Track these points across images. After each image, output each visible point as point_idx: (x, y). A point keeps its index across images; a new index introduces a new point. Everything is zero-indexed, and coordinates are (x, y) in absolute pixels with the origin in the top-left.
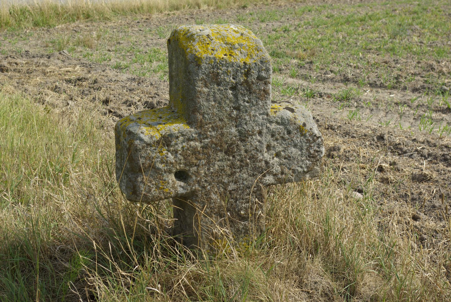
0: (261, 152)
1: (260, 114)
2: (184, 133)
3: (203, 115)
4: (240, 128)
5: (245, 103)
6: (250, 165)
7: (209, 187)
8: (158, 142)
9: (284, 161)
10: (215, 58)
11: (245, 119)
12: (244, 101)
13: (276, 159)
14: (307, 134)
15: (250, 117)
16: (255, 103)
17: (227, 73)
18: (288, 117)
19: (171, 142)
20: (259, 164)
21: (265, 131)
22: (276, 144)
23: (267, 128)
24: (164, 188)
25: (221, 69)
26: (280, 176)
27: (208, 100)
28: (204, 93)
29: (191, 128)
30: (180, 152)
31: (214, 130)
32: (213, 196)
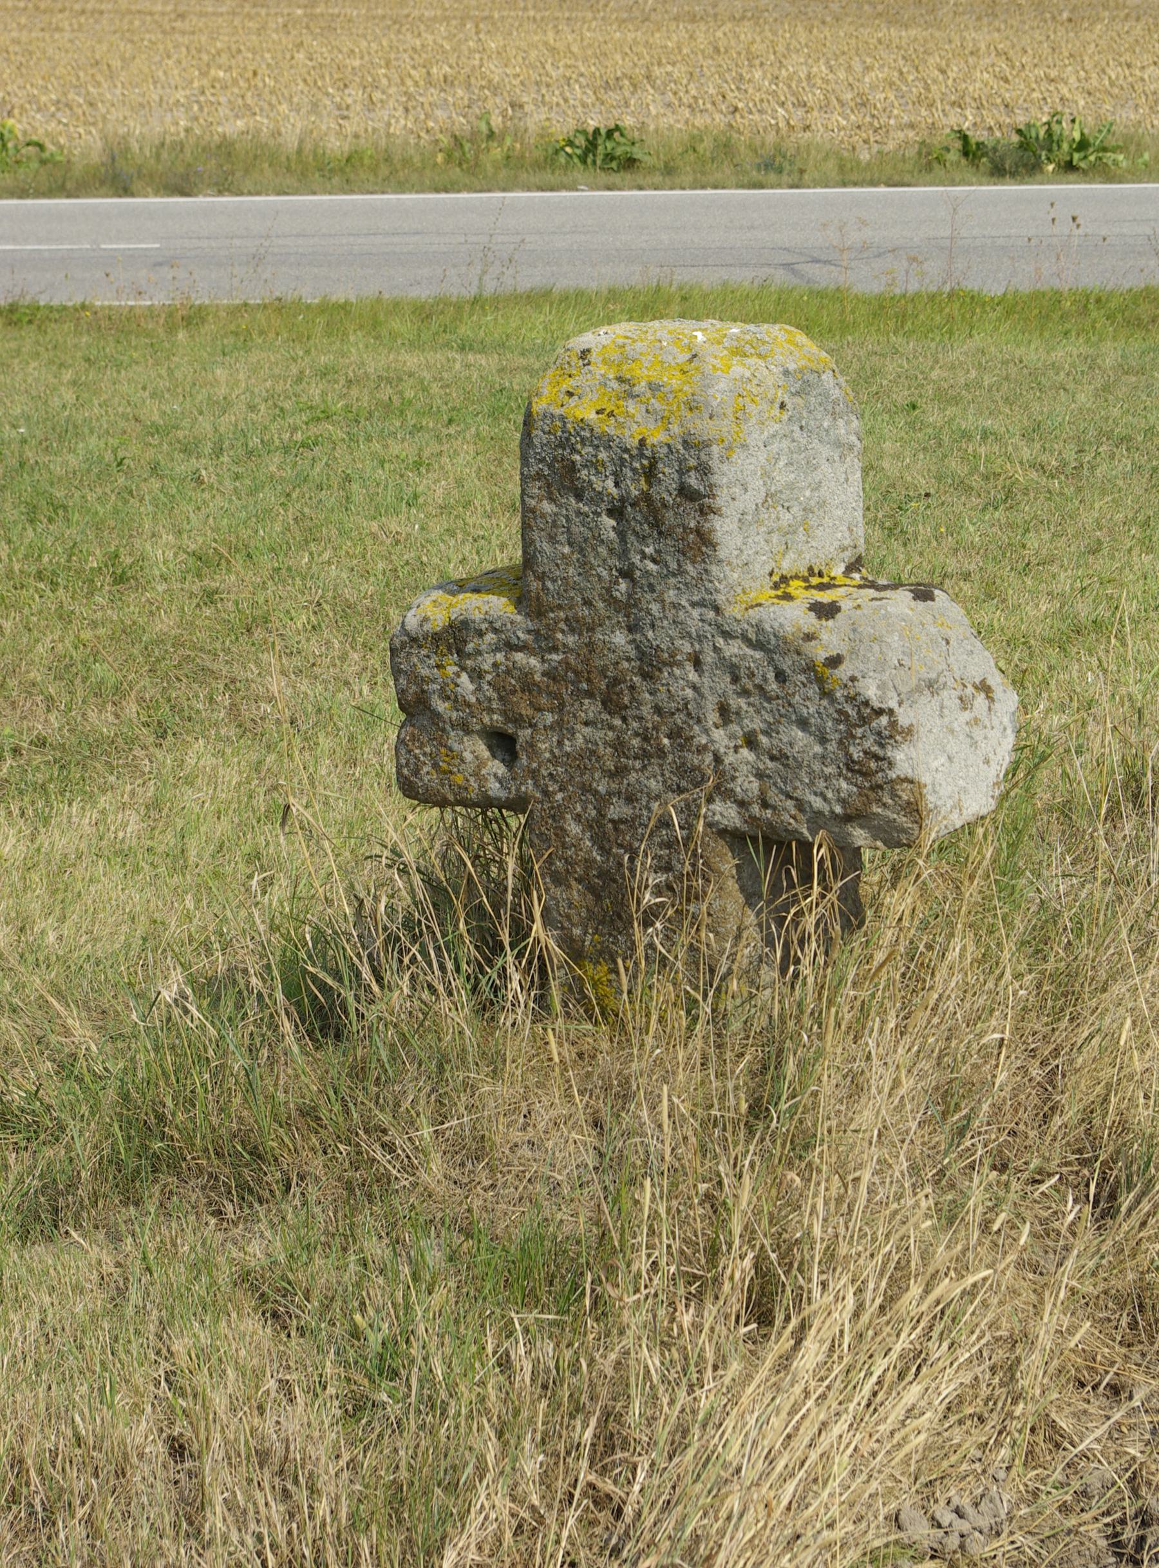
0: (699, 721)
1: (694, 605)
2: (497, 625)
3: (542, 577)
4: (638, 637)
5: (647, 562)
6: (670, 757)
7: (559, 796)
8: (436, 638)
9: (770, 764)
10: (562, 418)
11: (648, 612)
12: (644, 556)
13: (745, 752)
14: (838, 695)
15: (664, 608)
16: (673, 566)
17: (594, 464)
18: (776, 625)
19: (465, 642)
20: (694, 759)
21: (709, 657)
22: (744, 707)
23: (716, 649)
24: (451, 772)
25: (579, 453)
26: (756, 809)
27: (552, 539)
28: (543, 516)
29: (519, 613)
30: (489, 677)
31: (573, 631)
32: (574, 828)
